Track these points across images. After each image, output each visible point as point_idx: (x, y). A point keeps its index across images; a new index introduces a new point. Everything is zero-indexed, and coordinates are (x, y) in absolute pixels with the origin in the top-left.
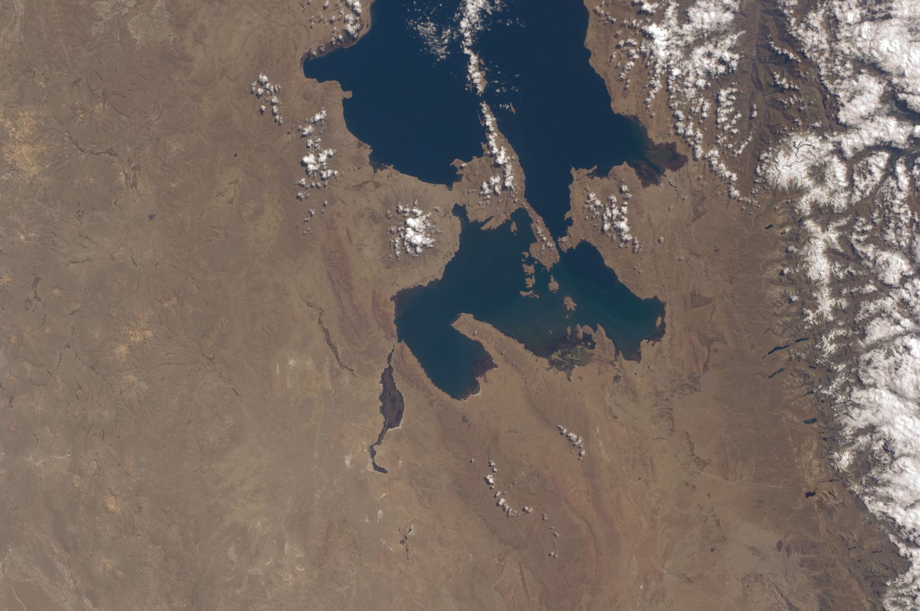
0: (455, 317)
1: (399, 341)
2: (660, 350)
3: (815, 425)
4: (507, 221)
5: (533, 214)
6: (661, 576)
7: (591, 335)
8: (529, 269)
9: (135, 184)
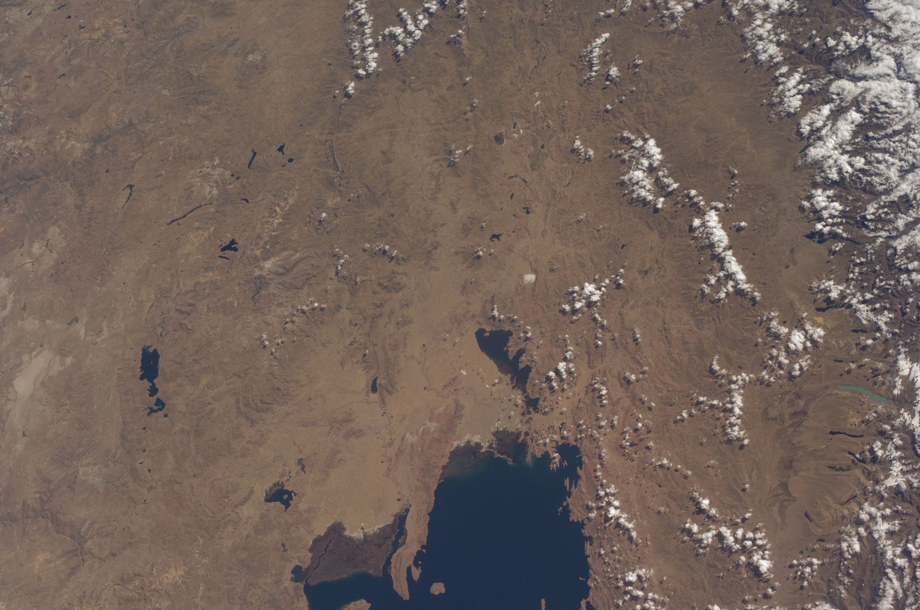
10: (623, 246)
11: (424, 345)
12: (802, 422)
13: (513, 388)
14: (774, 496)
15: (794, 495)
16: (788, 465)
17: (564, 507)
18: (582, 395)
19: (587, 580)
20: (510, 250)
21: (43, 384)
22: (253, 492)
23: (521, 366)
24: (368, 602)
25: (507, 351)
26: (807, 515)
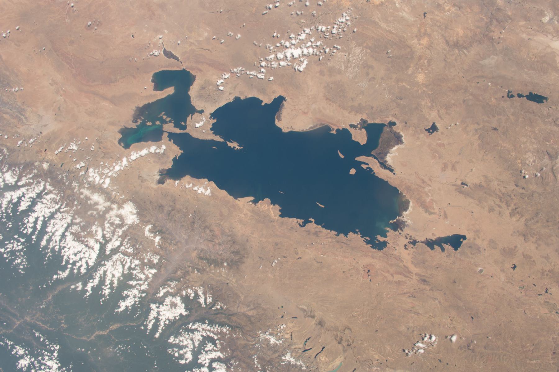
0: (175, 89)
1: (183, 69)
2: (115, 139)
3: (60, 165)
4: (186, 123)
5: (182, 131)
6: (61, 96)
7: (136, 123)
8: (168, 119)
9: (298, 23)
10: (472, 318)
11: (472, 212)
12: (336, 340)
13: (427, 239)
14: (311, 310)
16: (321, 323)
17: (358, 232)
18: (405, 263)
20: (502, 270)
21: (554, 52)
22: (441, 119)
23: (436, 247)
24: (363, 145)
25: (447, 244)
26: (296, 318)
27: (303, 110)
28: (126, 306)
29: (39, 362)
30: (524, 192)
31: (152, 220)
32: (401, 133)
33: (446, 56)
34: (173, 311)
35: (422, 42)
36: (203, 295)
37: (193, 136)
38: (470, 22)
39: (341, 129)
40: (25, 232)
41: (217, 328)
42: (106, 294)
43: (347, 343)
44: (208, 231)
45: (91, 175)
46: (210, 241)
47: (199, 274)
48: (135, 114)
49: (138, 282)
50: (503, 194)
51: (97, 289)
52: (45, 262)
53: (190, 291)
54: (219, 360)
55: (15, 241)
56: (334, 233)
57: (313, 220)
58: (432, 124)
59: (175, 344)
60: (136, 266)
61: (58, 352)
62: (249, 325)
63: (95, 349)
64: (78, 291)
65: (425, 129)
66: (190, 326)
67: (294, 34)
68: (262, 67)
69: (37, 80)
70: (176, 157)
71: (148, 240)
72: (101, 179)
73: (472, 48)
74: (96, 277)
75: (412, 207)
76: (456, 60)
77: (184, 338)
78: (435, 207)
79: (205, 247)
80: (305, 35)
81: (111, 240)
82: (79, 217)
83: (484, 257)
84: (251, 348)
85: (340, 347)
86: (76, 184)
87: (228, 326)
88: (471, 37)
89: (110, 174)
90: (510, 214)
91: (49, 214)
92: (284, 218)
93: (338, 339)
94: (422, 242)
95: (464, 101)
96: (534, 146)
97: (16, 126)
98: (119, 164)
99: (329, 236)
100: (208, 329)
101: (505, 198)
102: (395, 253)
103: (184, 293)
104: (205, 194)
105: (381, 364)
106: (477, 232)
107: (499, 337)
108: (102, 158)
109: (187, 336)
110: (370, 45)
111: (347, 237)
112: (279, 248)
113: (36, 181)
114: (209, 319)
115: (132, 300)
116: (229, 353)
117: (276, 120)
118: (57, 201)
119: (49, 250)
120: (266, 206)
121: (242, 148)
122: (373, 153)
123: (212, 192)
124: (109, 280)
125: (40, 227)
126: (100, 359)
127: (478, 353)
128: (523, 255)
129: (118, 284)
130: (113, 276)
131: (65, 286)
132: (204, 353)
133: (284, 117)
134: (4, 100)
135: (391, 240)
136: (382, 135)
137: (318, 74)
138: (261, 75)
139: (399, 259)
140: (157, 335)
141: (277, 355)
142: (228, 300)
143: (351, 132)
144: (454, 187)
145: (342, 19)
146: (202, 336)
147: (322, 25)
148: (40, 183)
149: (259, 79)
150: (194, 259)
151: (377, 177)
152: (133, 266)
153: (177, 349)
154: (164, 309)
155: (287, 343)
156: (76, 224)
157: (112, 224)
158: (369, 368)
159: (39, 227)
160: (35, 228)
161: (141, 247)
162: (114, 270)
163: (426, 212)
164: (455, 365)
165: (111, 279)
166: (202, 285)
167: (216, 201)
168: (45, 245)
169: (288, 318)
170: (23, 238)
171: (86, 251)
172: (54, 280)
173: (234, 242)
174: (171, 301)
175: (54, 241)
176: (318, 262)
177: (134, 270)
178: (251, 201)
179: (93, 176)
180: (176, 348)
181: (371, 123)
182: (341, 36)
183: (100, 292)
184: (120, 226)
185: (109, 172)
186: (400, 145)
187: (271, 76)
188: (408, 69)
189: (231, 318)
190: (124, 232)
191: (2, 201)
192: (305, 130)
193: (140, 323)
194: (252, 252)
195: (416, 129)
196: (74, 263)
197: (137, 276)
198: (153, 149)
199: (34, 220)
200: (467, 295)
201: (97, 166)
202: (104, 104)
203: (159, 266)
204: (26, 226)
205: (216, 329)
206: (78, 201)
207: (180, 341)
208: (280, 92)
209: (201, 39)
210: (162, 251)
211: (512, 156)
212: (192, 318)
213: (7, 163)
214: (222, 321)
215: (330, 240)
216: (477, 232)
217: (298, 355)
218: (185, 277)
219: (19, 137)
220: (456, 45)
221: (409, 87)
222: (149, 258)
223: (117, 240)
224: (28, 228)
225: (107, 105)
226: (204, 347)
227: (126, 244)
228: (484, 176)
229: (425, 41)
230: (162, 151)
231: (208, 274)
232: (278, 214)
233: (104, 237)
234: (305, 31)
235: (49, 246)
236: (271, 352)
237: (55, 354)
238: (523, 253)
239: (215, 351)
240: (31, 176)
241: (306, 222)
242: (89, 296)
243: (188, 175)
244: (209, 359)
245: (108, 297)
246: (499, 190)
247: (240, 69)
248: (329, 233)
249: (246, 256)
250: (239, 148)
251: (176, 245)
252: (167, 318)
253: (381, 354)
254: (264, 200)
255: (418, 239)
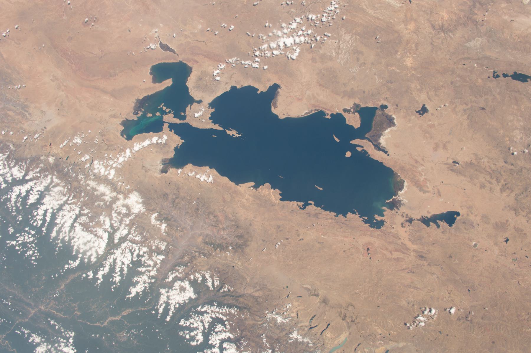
0: (173, 81)
1: (180, 61)
2: (118, 131)
3: (66, 159)
4: (186, 113)
5: (182, 122)
6: (63, 91)
7: (137, 115)
8: (168, 110)
9: (288, 13)
10: (469, 291)
11: (465, 189)
12: (340, 316)
13: (422, 216)
15: (311, 297)
16: (325, 301)
17: (356, 212)
18: (402, 241)
19: (321, 208)
20: (496, 244)
23: (431, 224)
24: (357, 128)
25: (442, 221)
26: (301, 297)
27: (298, 97)
28: (137, 292)
29: (56, 349)
30: (513, 168)
31: (158, 208)
32: (393, 116)
33: (432, 39)
34: (182, 295)
35: (409, 27)
36: (211, 278)
37: (193, 126)
38: (454, 6)
39: (335, 114)
40: (35, 224)
41: (225, 310)
42: (117, 281)
43: (350, 319)
44: (212, 217)
45: (96, 167)
46: (214, 226)
47: (205, 258)
48: (135, 106)
49: (147, 269)
50: (493, 171)
51: (108, 277)
52: (56, 253)
53: (197, 275)
54: (229, 340)
55: (26, 234)
56: (333, 214)
57: (313, 203)
58: (423, 106)
59: (186, 326)
60: (144, 253)
61: (73, 338)
62: (257, 306)
63: (109, 335)
64: (90, 279)
65: (416, 111)
66: (199, 308)
67: (285, 23)
68: (256, 56)
69: (39, 77)
70: (177, 147)
71: (154, 227)
72: (106, 170)
73: (457, 31)
74: (106, 265)
75: (406, 186)
76: (442, 43)
77: (194, 321)
78: (428, 186)
79: (210, 233)
80: (296, 24)
81: (118, 229)
82: (86, 208)
83: (478, 232)
84: (259, 328)
85: (345, 323)
86: (82, 176)
87: (236, 307)
88: (456, 20)
89: (114, 166)
90: (501, 190)
91: (58, 206)
92: (284, 202)
93: (342, 315)
94: (418, 220)
95: (452, 83)
96: (520, 123)
97: (21, 122)
98: (123, 155)
99: (329, 217)
100: (217, 311)
101: (495, 175)
102: (393, 231)
103: (192, 277)
104: (208, 181)
105: (384, 337)
106: (470, 208)
107: (495, 308)
108: (105, 150)
109: (197, 319)
110: (359, 32)
111: (346, 218)
112: (281, 231)
113: (43, 175)
114: (217, 302)
115: (143, 286)
116: (238, 333)
117: (273, 107)
118: (65, 193)
119: (59, 241)
120: (267, 191)
121: (241, 135)
122: (366, 136)
123: (214, 179)
124: (119, 267)
125: (50, 219)
126: (114, 343)
127: (476, 323)
128: (515, 228)
129: (128, 271)
130: (123, 263)
131: (77, 275)
132: (214, 334)
133: (280, 104)
134: (8, 97)
135: (388, 219)
136: (375, 119)
137: (310, 61)
138: (255, 64)
139: (396, 236)
140: (168, 319)
141: (284, 333)
142: (235, 282)
143: (344, 116)
144: (447, 166)
145: (331, 7)
146: (211, 317)
147: (312, 14)
148: (46, 176)
149: (254, 68)
150: (199, 244)
151: (372, 159)
152: (141, 253)
153: (188, 331)
154: (173, 294)
155: (293, 322)
156: (84, 215)
157: (119, 214)
158: (373, 342)
159: (48, 219)
160: (44, 220)
161: (148, 234)
162: (123, 258)
163: (420, 191)
164: (455, 336)
165: (120, 267)
166: (209, 269)
167: (219, 188)
168: (55, 236)
169: (294, 297)
170: (33, 231)
171: (96, 241)
172: (65, 270)
173: (238, 227)
174: (180, 285)
175: (64, 232)
176: (319, 243)
177: (143, 257)
178: (252, 186)
179: (98, 168)
180: (187, 330)
181: (363, 107)
182: (331, 24)
183: (111, 279)
184: (127, 215)
185: (114, 163)
186: (392, 127)
187: (265, 65)
188: (397, 54)
189: (238, 299)
190: (131, 220)
191: (11, 195)
192: (300, 116)
193: (151, 307)
194: (256, 235)
195: (407, 111)
196: (85, 253)
197: (146, 263)
198: (155, 140)
199: (43, 212)
200: (463, 269)
201: (101, 158)
202: (105, 97)
203: (166, 252)
204: (35, 218)
205: (224, 311)
206: (85, 192)
207: (191, 323)
208: (274, 80)
209: (196, 32)
210: (169, 238)
211: (500, 134)
212: (201, 301)
213: (15, 159)
214: (230, 303)
215: (330, 221)
216: (470, 208)
217: (304, 332)
218: (192, 261)
219: (25, 133)
220: (442, 29)
221: (398, 71)
222: (157, 245)
223: (125, 228)
224: (38, 220)
225: (108, 98)
226: (214, 328)
227: (133, 232)
228: (474, 154)
229: (411, 26)
230: (164, 142)
231: (214, 258)
232: (279, 198)
233: (112, 226)
234: (296, 20)
235: (59, 237)
236: (279, 331)
237: (71, 341)
238: (514, 226)
239: (225, 332)
240: (38, 170)
241: (306, 205)
242: (100, 283)
243: (190, 163)
244: (219, 340)
245: (118, 284)
246: (489, 166)
247: (235, 59)
248: (329, 215)
249: (250, 239)
250: (238, 135)
251: (181, 231)
252: (177, 302)
253: (383, 329)
254: (265, 185)
255: (414, 217)
